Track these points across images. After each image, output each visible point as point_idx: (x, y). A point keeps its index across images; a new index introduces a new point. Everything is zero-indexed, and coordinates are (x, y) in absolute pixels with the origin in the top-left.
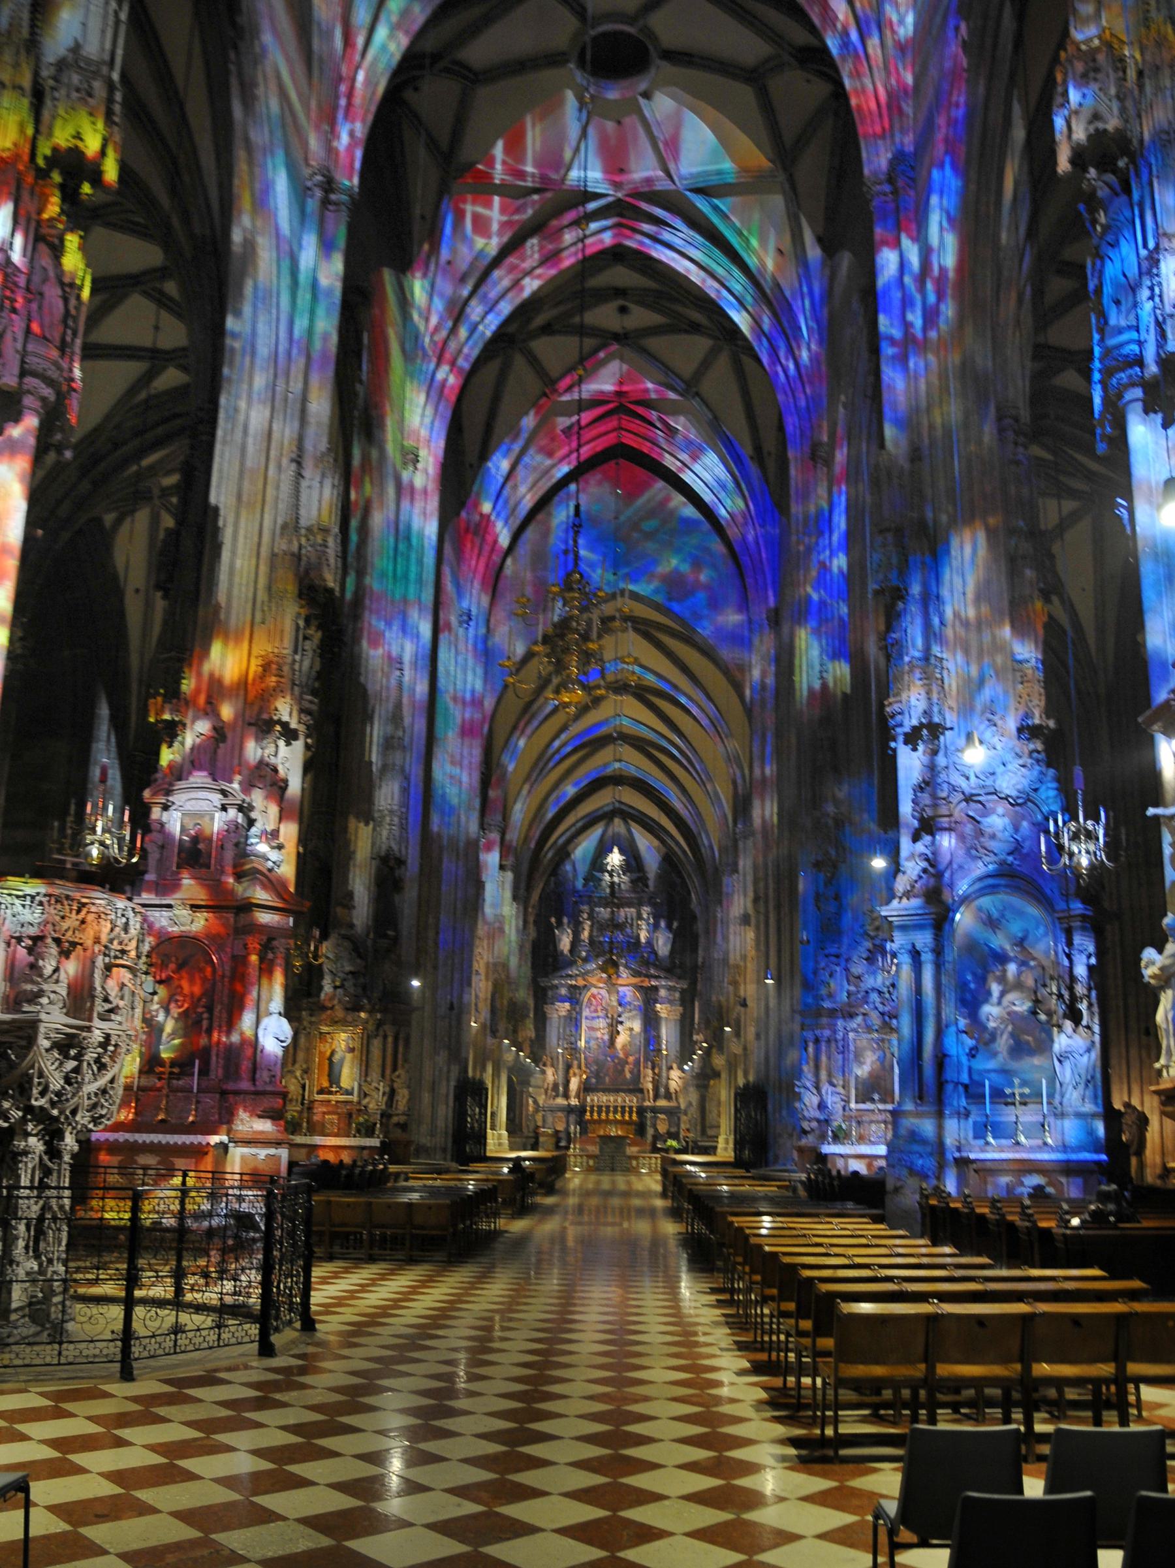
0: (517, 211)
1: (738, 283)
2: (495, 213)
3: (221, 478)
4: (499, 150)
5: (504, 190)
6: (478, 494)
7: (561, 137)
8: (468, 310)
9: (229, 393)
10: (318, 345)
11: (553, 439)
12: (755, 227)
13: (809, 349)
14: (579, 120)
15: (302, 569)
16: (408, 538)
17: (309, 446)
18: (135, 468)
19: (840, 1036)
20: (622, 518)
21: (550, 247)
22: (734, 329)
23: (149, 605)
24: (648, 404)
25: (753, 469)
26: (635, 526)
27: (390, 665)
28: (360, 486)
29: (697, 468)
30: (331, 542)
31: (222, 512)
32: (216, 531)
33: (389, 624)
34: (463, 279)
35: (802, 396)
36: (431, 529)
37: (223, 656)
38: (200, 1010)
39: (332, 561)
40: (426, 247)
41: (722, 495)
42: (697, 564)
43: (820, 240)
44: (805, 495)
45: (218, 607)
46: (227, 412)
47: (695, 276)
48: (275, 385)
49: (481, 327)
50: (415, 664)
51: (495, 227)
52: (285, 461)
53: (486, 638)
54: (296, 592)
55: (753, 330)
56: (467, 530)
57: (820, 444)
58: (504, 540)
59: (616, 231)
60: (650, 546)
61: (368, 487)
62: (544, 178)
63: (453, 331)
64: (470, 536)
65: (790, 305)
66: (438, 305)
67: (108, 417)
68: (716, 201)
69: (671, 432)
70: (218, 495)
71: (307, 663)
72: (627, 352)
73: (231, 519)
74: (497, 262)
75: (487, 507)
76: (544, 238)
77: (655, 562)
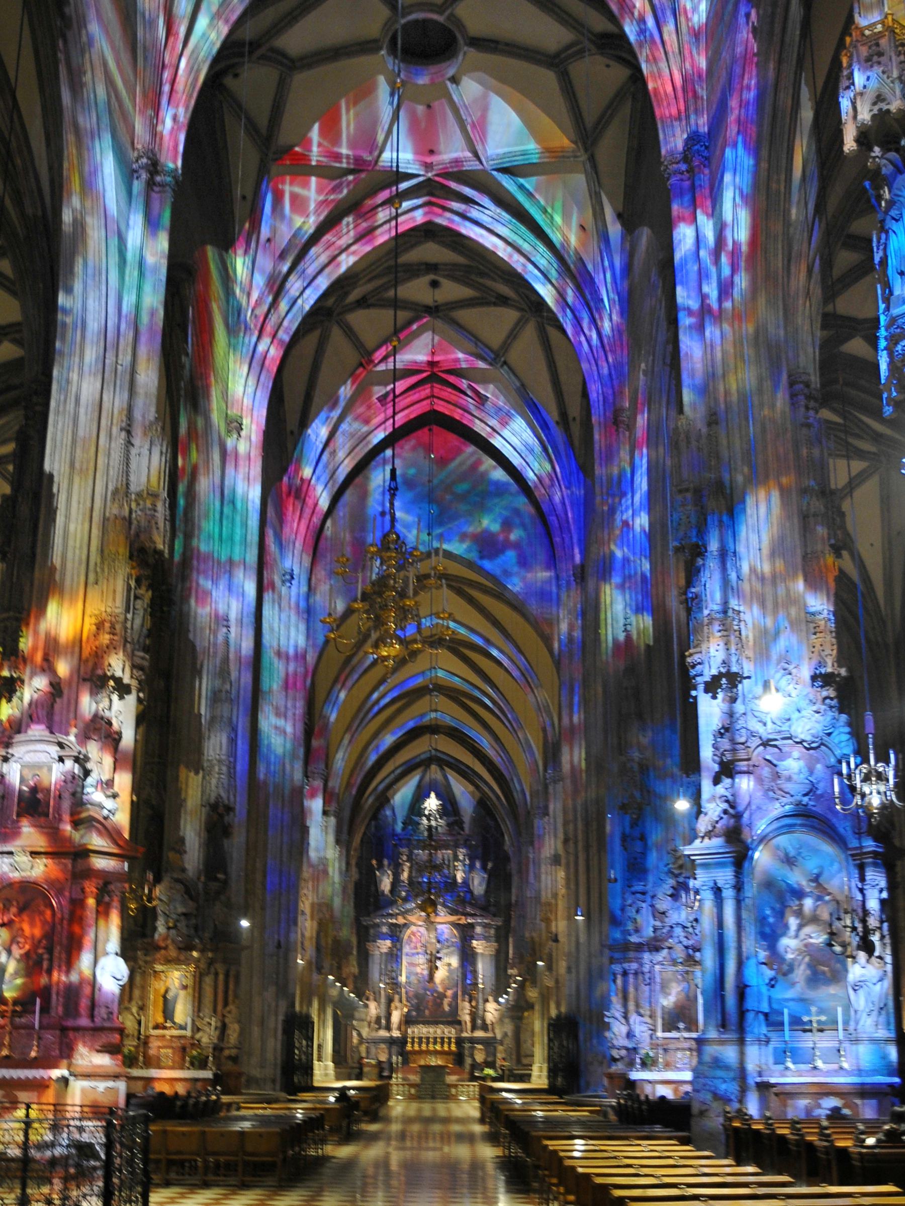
0: (334, 190)
1: (543, 257)
3: (54, 446)
4: (315, 134)
7: (375, 123)
8: (288, 285)
10: (145, 319)
11: (369, 407)
12: (558, 205)
13: (611, 320)
15: (132, 532)
16: (233, 502)
17: (137, 415)
20: (435, 481)
22: (539, 303)
25: (558, 432)
28: (186, 453)
29: (506, 433)
30: (160, 507)
31: (56, 479)
32: (51, 496)
33: (215, 582)
34: (282, 256)
35: (605, 365)
36: (255, 493)
37: (59, 615)
39: (161, 525)
40: (247, 225)
41: (530, 459)
42: (507, 525)
43: (620, 216)
44: (609, 456)
45: (53, 569)
47: (502, 251)
49: (300, 301)
50: (240, 622)
51: (312, 206)
52: (115, 430)
55: (557, 301)
57: (622, 409)
58: (324, 503)
59: (426, 209)
60: (462, 507)
61: (194, 454)
62: (358, 160)
63: (274, 304)
64: (291, 500)
65: (592, 279)
66: (259, 280)
69: (481, 400)
70: (52, 462)
71: (138, 622)
72: (439, 323)
74: (314, 239)
75: (307, 472)
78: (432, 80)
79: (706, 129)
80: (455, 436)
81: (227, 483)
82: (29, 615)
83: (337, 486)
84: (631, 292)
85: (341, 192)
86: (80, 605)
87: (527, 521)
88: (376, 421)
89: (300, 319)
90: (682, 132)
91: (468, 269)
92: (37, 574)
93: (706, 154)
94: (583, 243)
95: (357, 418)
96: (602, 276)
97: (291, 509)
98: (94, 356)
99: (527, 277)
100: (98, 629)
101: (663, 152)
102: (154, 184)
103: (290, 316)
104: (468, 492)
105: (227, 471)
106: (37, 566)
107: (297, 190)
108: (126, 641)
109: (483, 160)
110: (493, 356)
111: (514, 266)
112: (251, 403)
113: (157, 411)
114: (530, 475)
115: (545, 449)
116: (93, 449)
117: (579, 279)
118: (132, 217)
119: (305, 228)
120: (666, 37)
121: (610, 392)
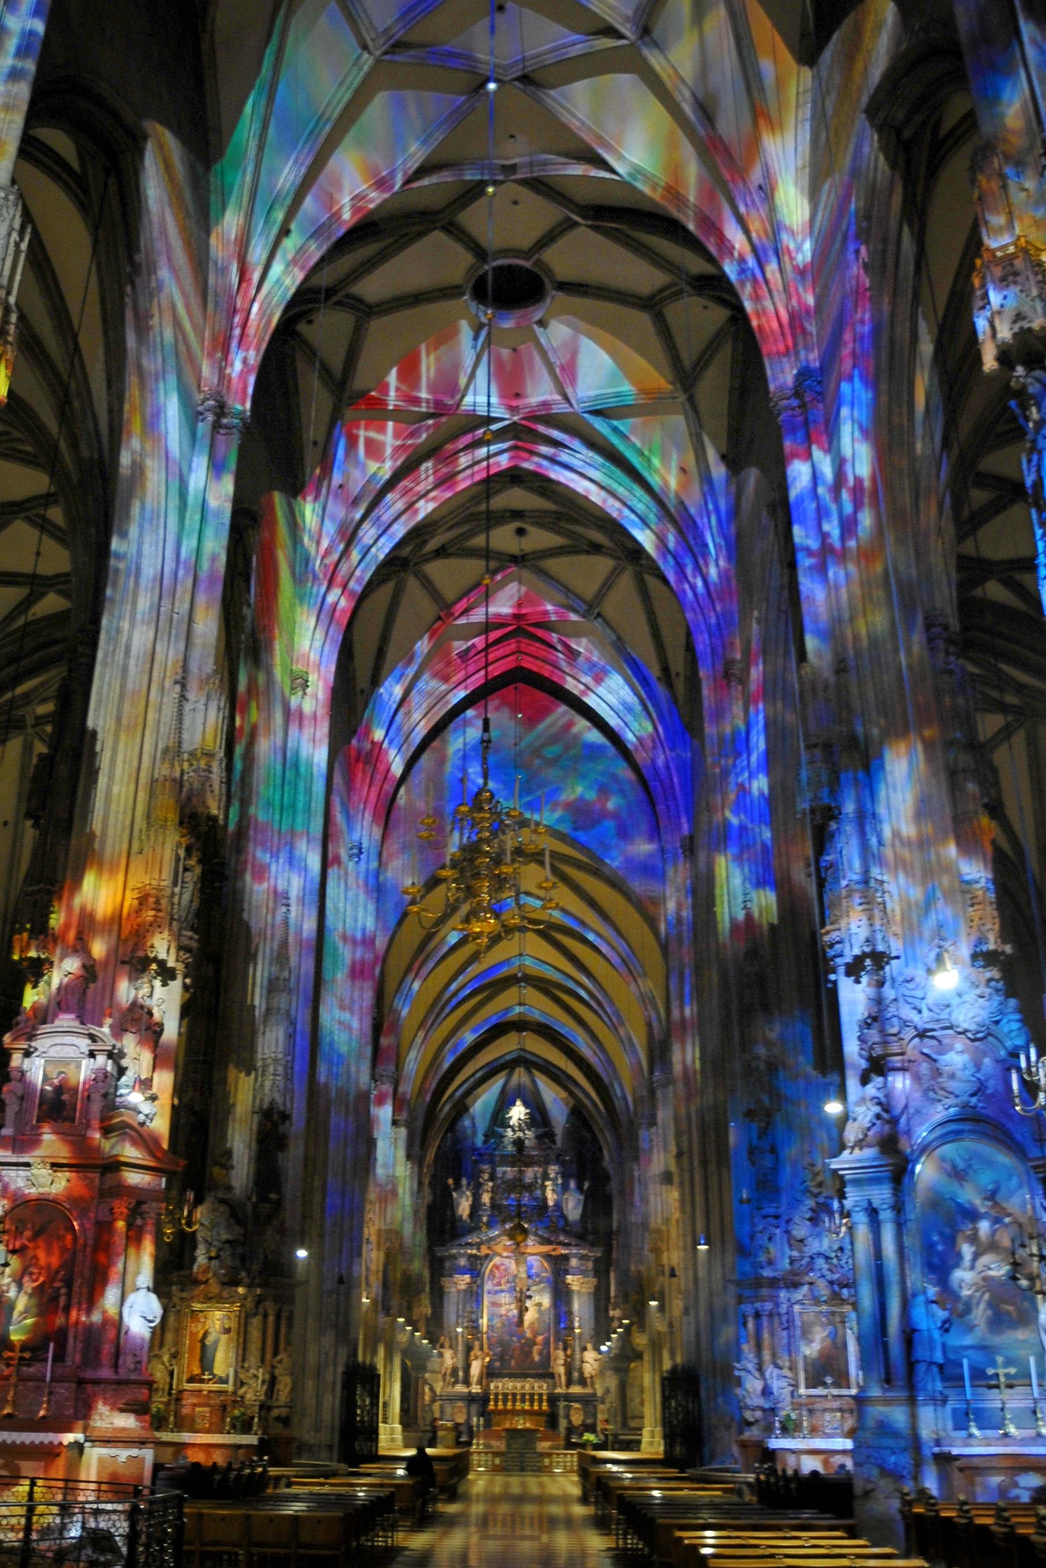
0: (412, 435)
1: (641, 501)
2: (388, 437)
3: (99, 701)
4: (392, 378)
5: (397, 415)
6: (370, 720)
7: (457, 367)
8: (361, 533)
9: (112, 614)
10: (205, 565)
11: (448, 664)
12: (656, 445)
13: (717, 565)
14: (474, 347)
16: (296, 766)
17: (193, 667)
19: (783, 1309)
20: (523, 744)
21: (445, 470)
22: (636, 551)
25: (661, 690)
26: (537, 752)
27: (275, 901)
28: (245, 711)
29: (601, 690)
30: (215, 767)
31: (100, 736)
32: (93, 755)
33: (275, 855)
34: (355, 502)
35: (712, 614)
36: (320, 756)
37: (96, 889)
38: (57, 1284)
41: (629, 718)
42: (603, 791)
43: (724, 457)
44: (719, 713)
45: (92, 836)
46: (108, 632)
47: (596, 496)
48: (159, 606)
49: (373, 550)
50: (302, 900)
51: (388, 451)
52: (168, 683)
53: (377, 874)
54: (177, 820)
55: (658, 548)
56: (358, 759)
57: (733, 662)
58: (397, 768)
60: (553, 773)
61: (254, 715)
62: (438, 403)
63: (346, 553)
64: (360, 765)
65: (695, 522)
66: (330, 528)
68: (615, 423)
69: (572, 655)
70: (97, 718)
71: (187, 897)
72: (526, 574)
73: (109, 744)
75: (378, 734)
76: (438, 462)
77: (557, 790)
78: (518, 323)
79: (817, 364)
80: (545, 695)
81: (289, 745)
82: (62, 888)
83: (412, 749)
84: (739, 535)
85: (420, 436)
86: (121, 877)
87: (627, 787)
88: (455, 679)
89: (373, 568)
90: (792, 368)
91: (558, 516)
92: (74, 841)
93: (818, 389)
94: (684, 485)
95: (435, 675)
96: (705, 520)
97: (360, 775)
98: (148, 605)
99: (624, 522)
100: (141, 904)
101: (772, 387)
102: (220, 426)
103: (362, 565)
104: (560, 756)
105: (290, 732)
106: (74, 834)
107: (373, 435)
108: (172, 919)
109: (573, 402)
110: (585, 607)
111: (609, 510)
112: (318, 658)
113: (216, 663)
114: (630, 737)
115: (645, 708)
116: (143, 703)
117: (681, 523)
118: (195, 459)
119: (381, 474)
120: (769, 275)
121: (719, 643)
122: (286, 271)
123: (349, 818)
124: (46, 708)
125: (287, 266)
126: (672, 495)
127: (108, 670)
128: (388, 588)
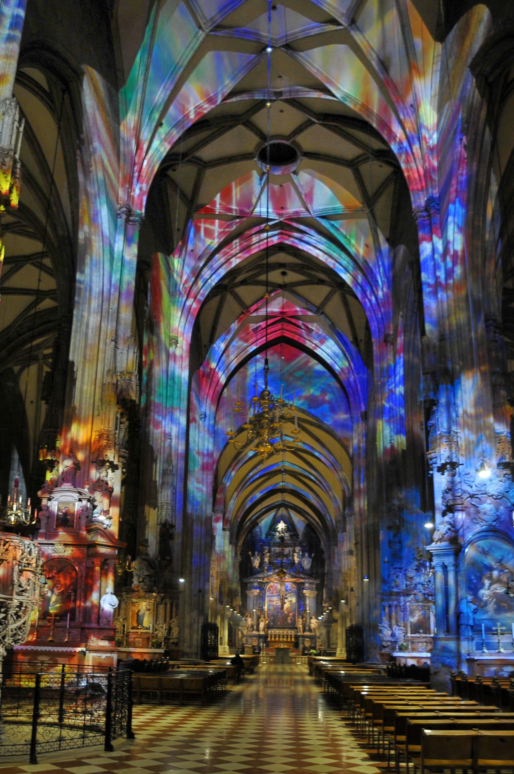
0: (228, 227)
1: (345, 260)
2: (216, 227)
3: (75, 348)
4: (218, 199)
5: (220, 217)
6: (209, 359)
7: (251, 194)
8: (203, 273)
9: (78, 309)
10: (124, 287)
11: (248, 334)
12: (353, 233)
13: (383, 291)
14: (260, 184)
15: (118, 391)
16: (173, 379)
17: (121, 333)
18: (29, 345)
20: (284, 371)
21: (245, 244)
22: (343, 283)
23: (38, 409)
24: (297, 317)
25: (353, 347)
26: (291, 374)
27: (165, 437)
28: (147, 353)
29: (323, 347)
30: (133, 378)
31: (76, 364)
32: (73, 373)
33: (164, 417)
34: (200, 258)
35: (379, 313)
36: (185, 374)
37: (78, 431)
39: (134, 387)
40: (180, 243)
41: (337, 360)
42: (324, 392)
43: (388, 240)
44: (381, 358)
45: (74, 408)
46: (77, 317)
47: (322, 257)
48: (102, 306)
49: (209, 281)
50: (178, 437)
51: (216, 234)
52: (108, 341)
53: (214, 426)
54: (116, 402)
55: (353, 282)
56: (203, 376)
57: (389, 335)
58: (223, 380)
59: (279, 236)
60: (299, 383)
61: (152, 355)
62: (241, 211)
63: (195, 282)
64: (205, 379)
65: (372, 270)
66: (187, 270)
67: (15, 321)
68: (333, 222)
69: (309, 331)
70: (74, 356)
71: (122, 435)
72: (286, 293)
73: (80, 368)
74: (217, 250)
75: (213, 365)
76: (242, 240)
77: (301, 391)
78: (283, 173)
79: (438, 195)
80: (295, 349)
81: (169, 369)
82: (61, 430)
83: (230, 372)
84: (394, 277)
85: (232, 227)
86: (90, 426)
87: (335, 390)
88: (251, 341)
89: (209, 289)
90: (424, 197)
91: (303, 266)
92: (66, 410)
93: (437, 207)
94: (367, 253)
95: (241, 339)
96: (377, 269)
97: (205, 383)
98: (96, 305)
99: (336, 270)
100: (100, 437)
101: (414, 206)
102: (129, 221)
103: (204, 288)
104: (303, 376)
105: (170, 363)
106: (66, 407)
107: (208, 226)
108: (115, 444)
109: (311, 212)
110: (316, 309)
111: (329, 264)
112: (182, 330)
113: (132, 332)
114: (337, 368)
115: (345, 355)
116: (96, 349)
117: (365, 271)
118: (117, 236)
119: (212, 245)
120: (414, 150)
121: (382, 326)
122: (161, 144)
123: (199, 402)
124: (49, 351)
125: (161, 141)
126: (361, 258)
127: (78, 335)
128: (217, 299)
